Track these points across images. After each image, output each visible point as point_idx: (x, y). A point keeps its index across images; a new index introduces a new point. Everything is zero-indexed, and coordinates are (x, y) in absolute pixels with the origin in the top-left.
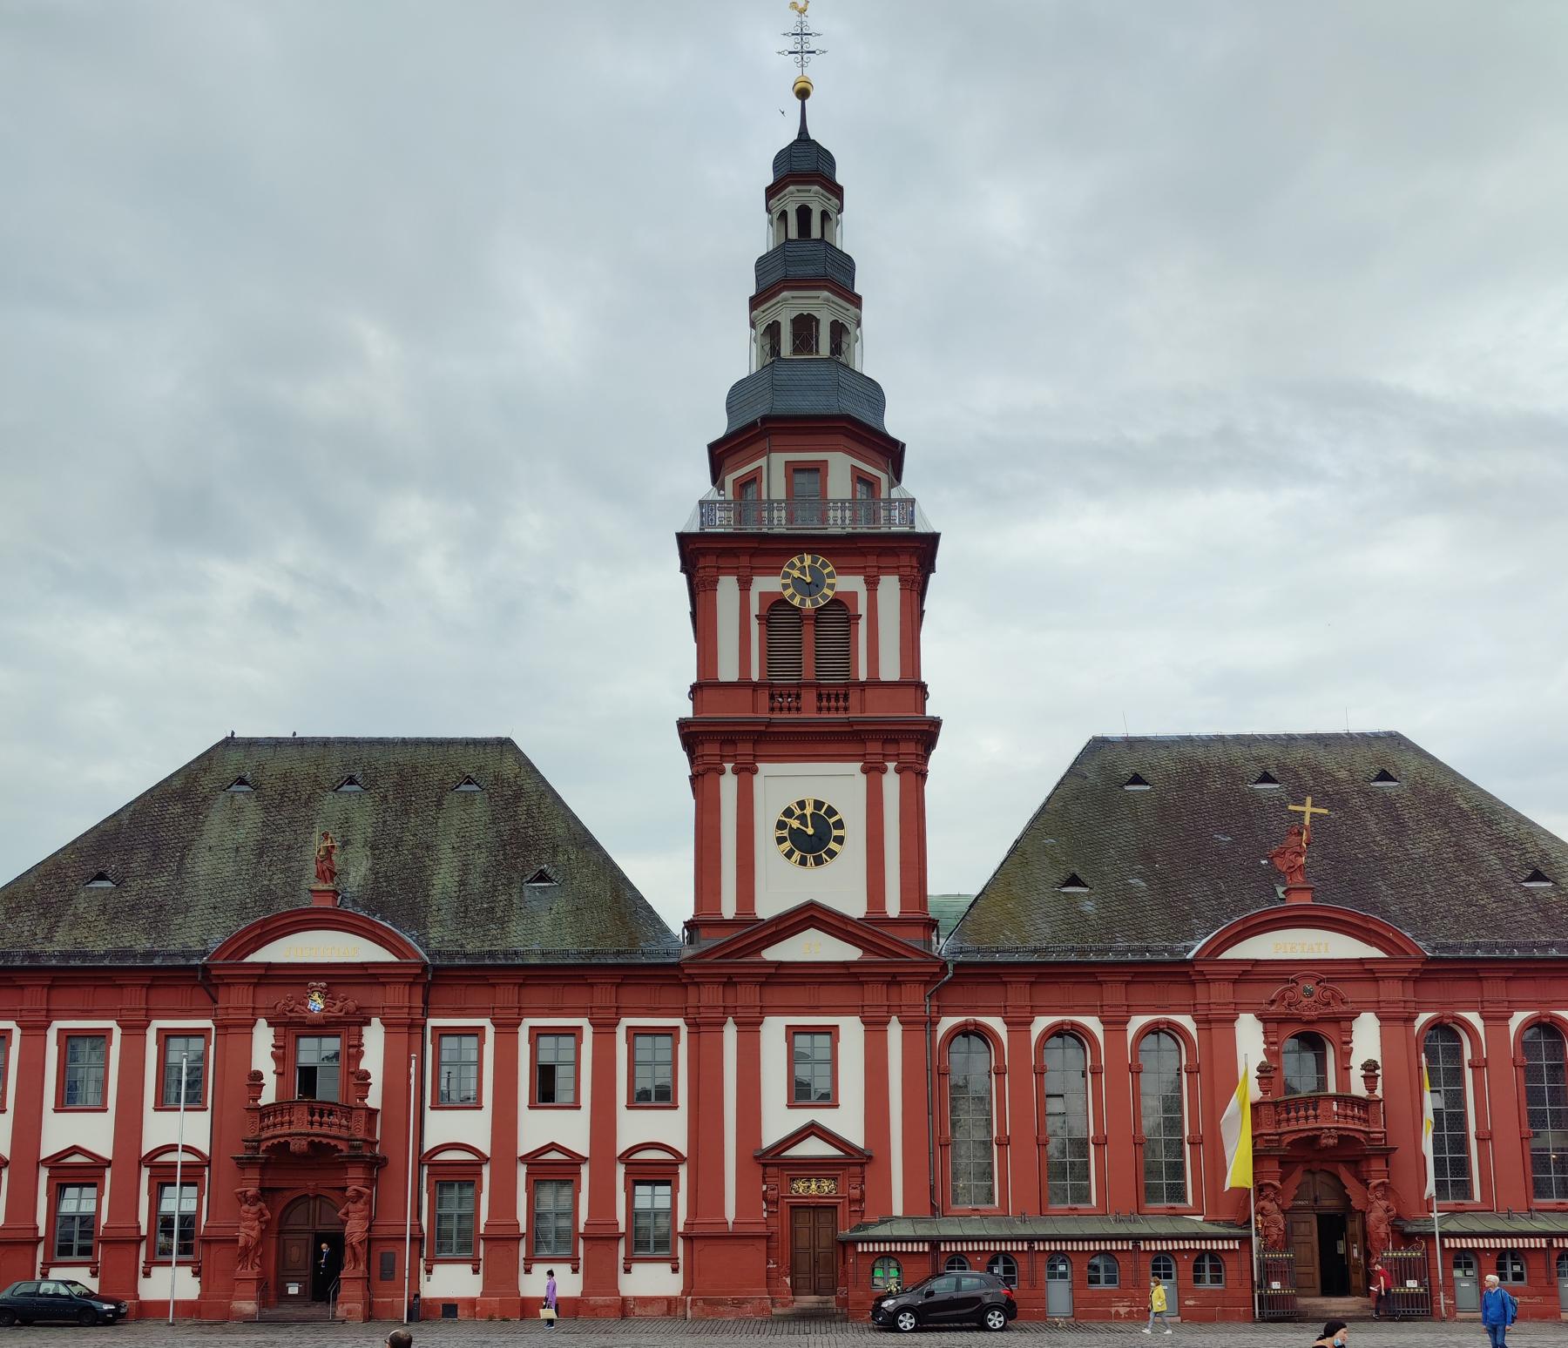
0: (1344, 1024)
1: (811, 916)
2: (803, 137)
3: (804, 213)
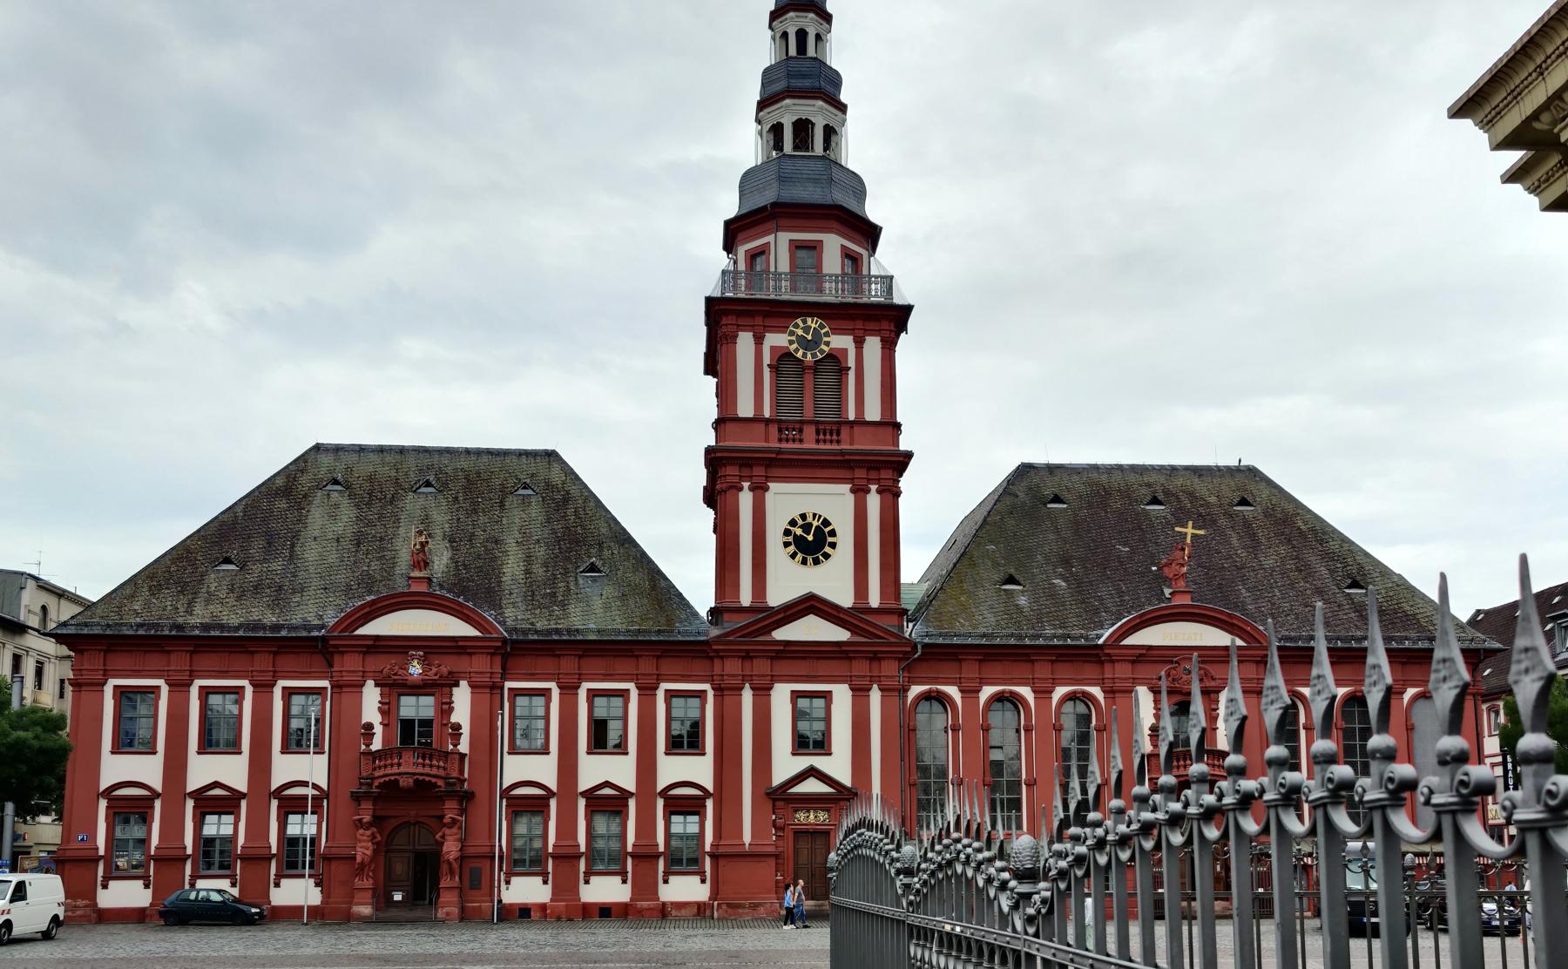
1: (811, 605)
3: (802, 35)
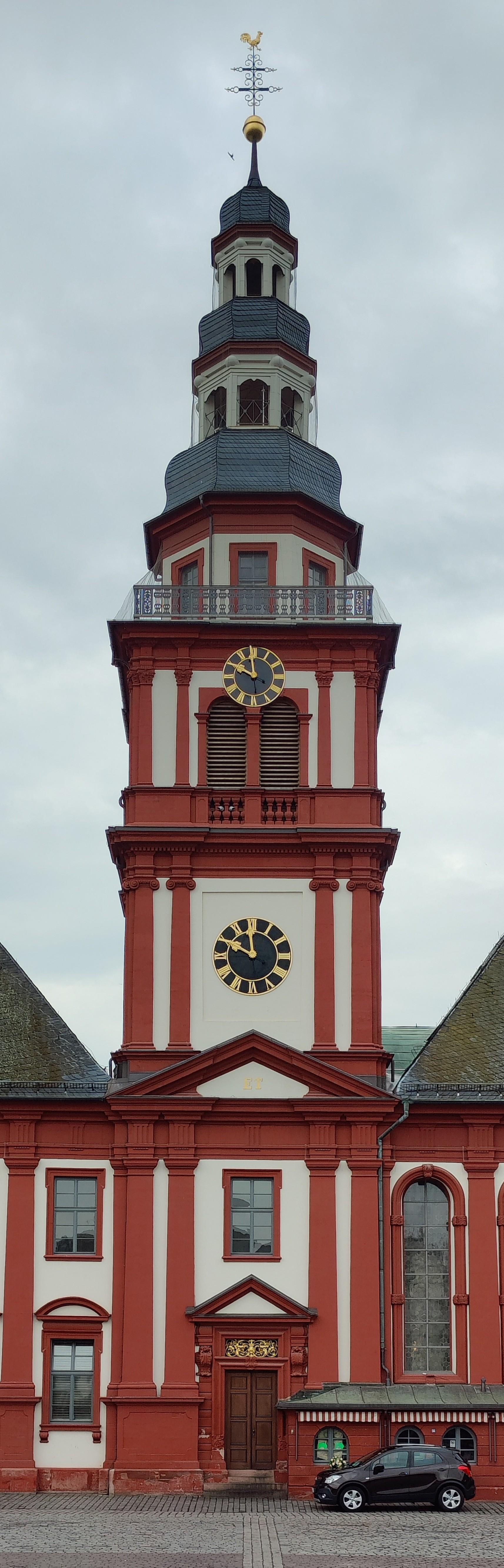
2: (254, 183)
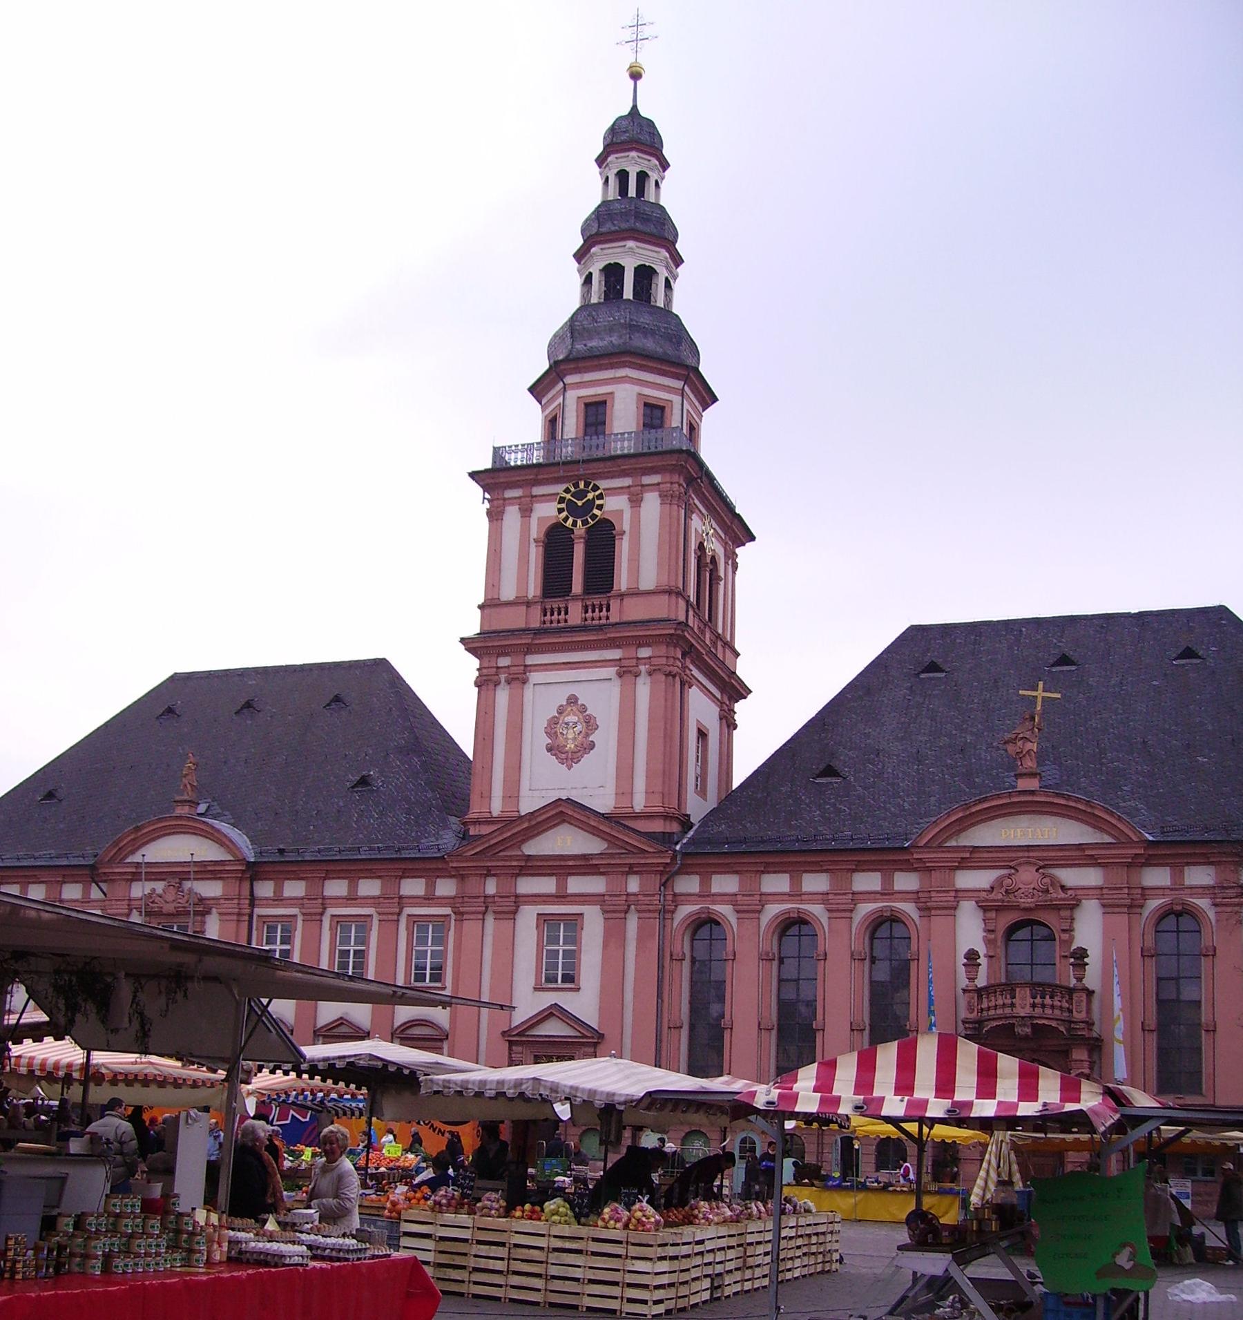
0: (1064, 913)
